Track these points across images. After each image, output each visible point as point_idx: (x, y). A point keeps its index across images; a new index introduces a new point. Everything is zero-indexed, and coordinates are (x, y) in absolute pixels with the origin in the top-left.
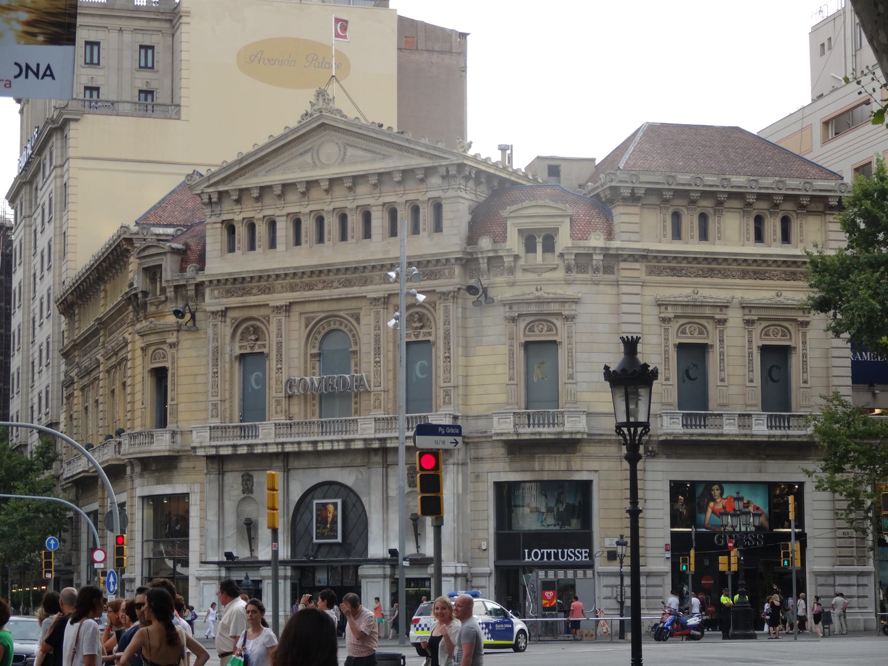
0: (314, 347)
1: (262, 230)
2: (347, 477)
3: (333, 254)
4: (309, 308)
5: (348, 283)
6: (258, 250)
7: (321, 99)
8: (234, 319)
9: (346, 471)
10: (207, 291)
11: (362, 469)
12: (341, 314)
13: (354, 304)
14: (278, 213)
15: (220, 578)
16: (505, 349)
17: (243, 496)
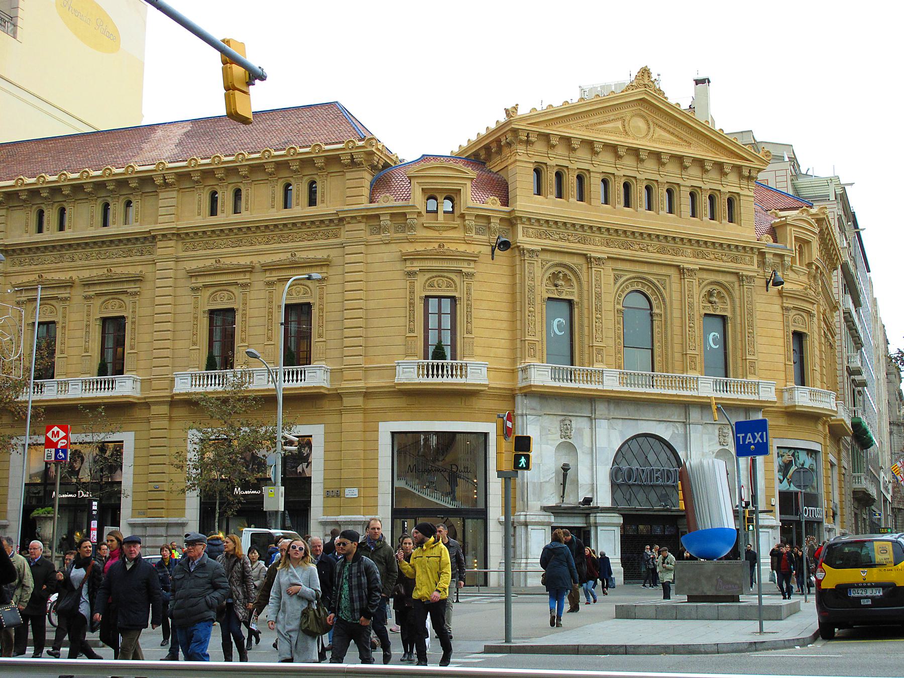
0: (618, 303)
1: (571, 181)
2: (665, 432)
3: (638, 218)
4: (620, 266)
5: (662, 250)
6: (571, 200)
7: (646, 75)
8: (548, 261)
9: (663, 425)
10: (520, 228)
11: (677, 424)
12: (649, 277)
13: (663, 271)
14: (592, 169)
15: (548, 524)
16: (780, 334)
17: (564, 440)
